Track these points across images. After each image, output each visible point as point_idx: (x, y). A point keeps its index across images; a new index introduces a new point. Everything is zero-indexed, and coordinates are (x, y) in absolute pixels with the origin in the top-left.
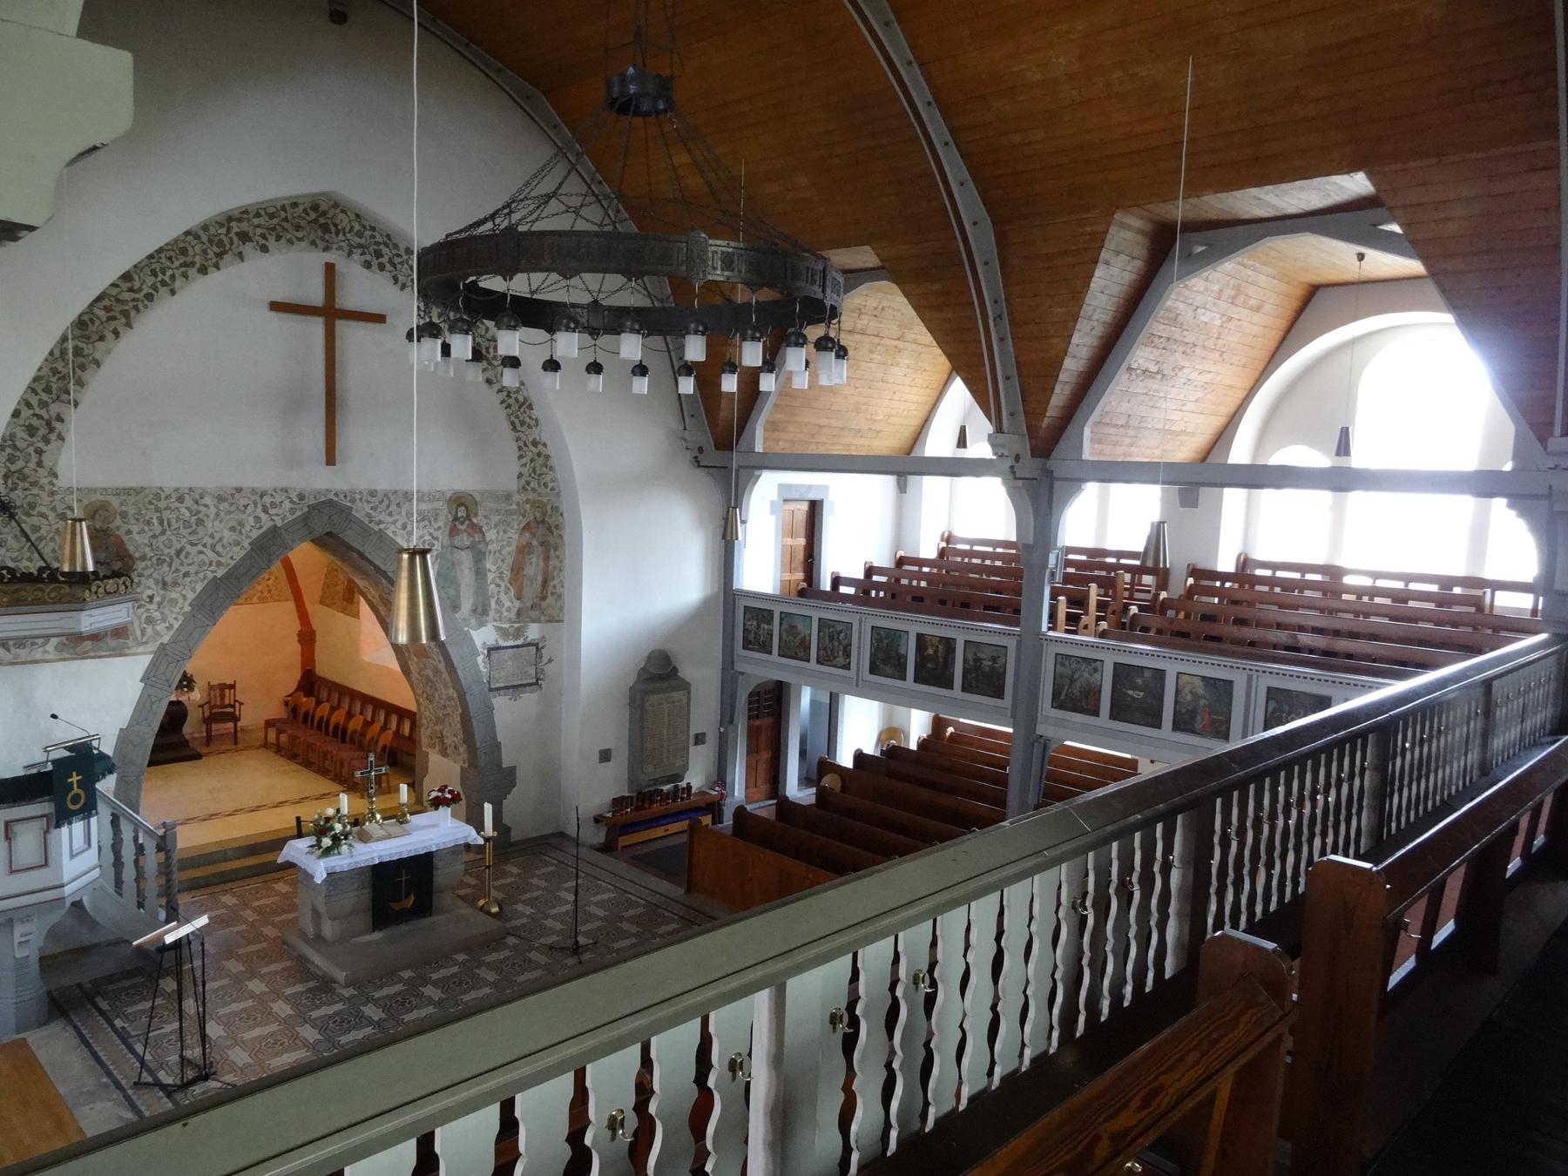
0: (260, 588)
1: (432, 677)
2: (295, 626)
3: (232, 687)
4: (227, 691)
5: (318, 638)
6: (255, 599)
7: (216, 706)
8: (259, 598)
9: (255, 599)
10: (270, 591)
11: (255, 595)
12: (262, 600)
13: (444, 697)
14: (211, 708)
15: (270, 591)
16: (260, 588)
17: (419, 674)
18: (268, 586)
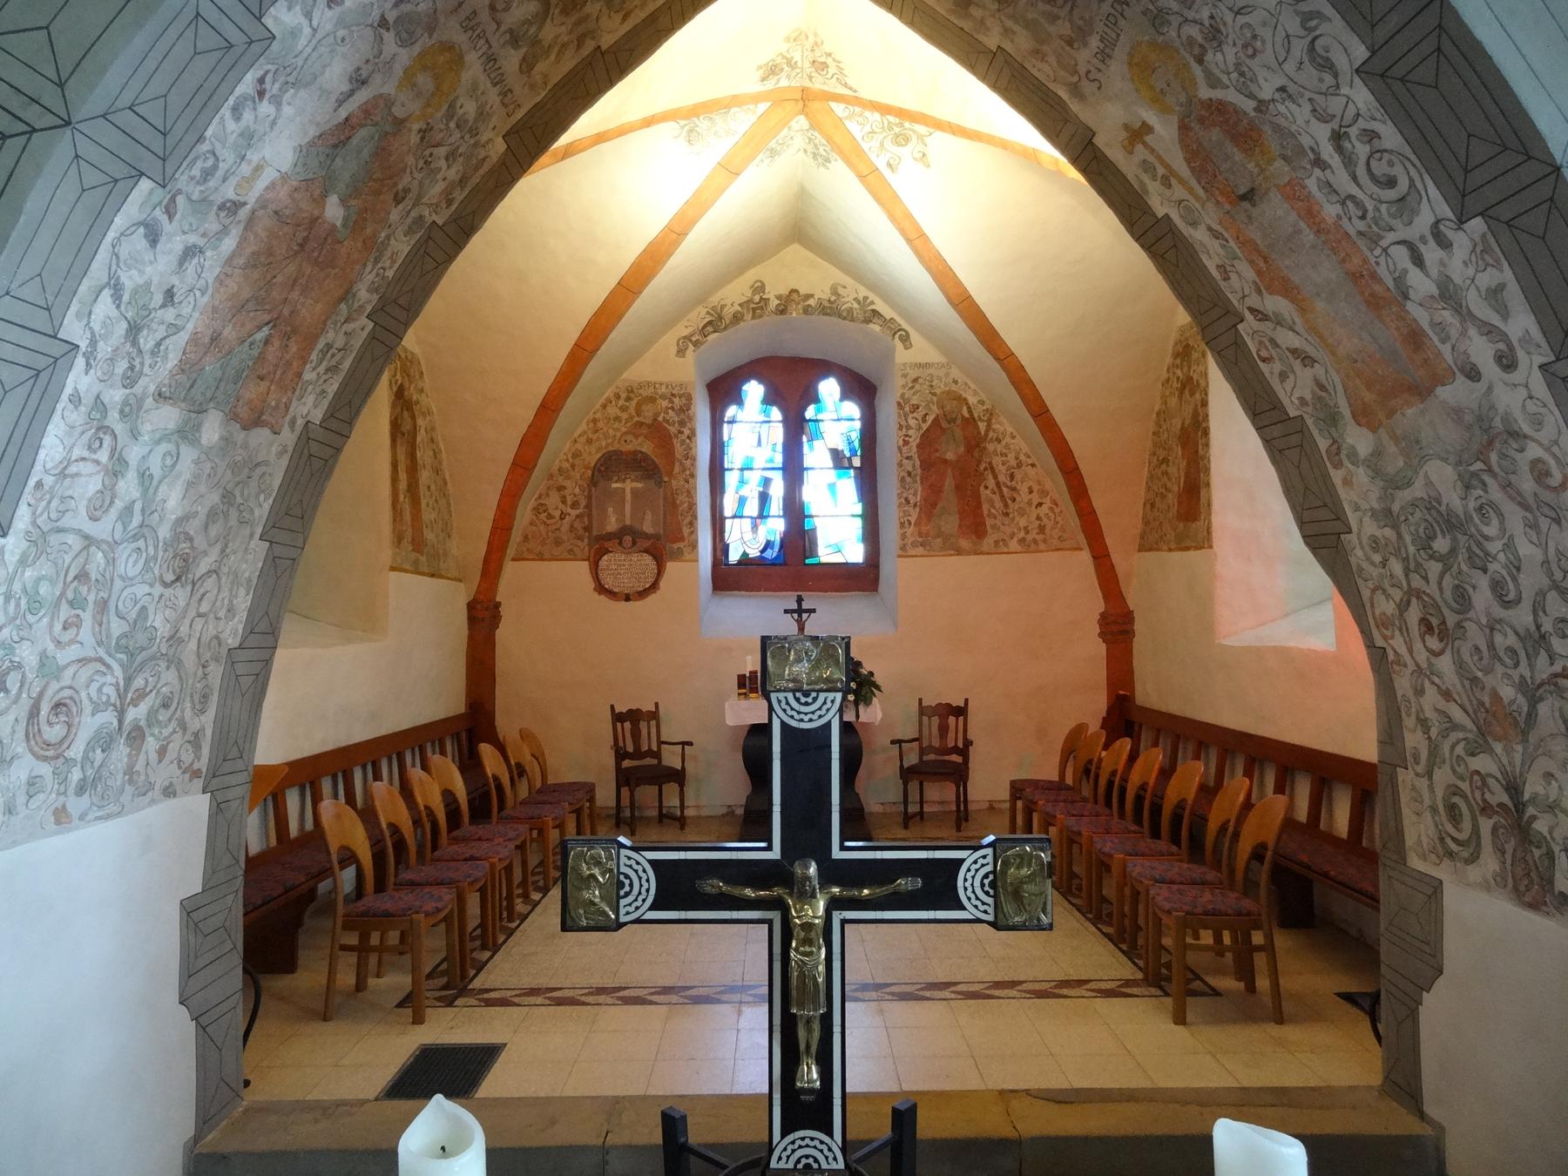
0: (1023, 522)
1: (1453, 499)
2: (1098, 605)
3: (961, 712)
4: (952, 720)
5: (1139, 626)
6: (1014, 545)
7: (931, 749)
8: (1022, 541)
9: (1014, 545)
10: (1042, 529)
11: (1012, 536)
12: (1027, 546)
13: (1531, 581)
14: (922, 751)
15: (1042, 529)
16: (1023, 522)
17: (1386, 516)
18: (1038, 518)
